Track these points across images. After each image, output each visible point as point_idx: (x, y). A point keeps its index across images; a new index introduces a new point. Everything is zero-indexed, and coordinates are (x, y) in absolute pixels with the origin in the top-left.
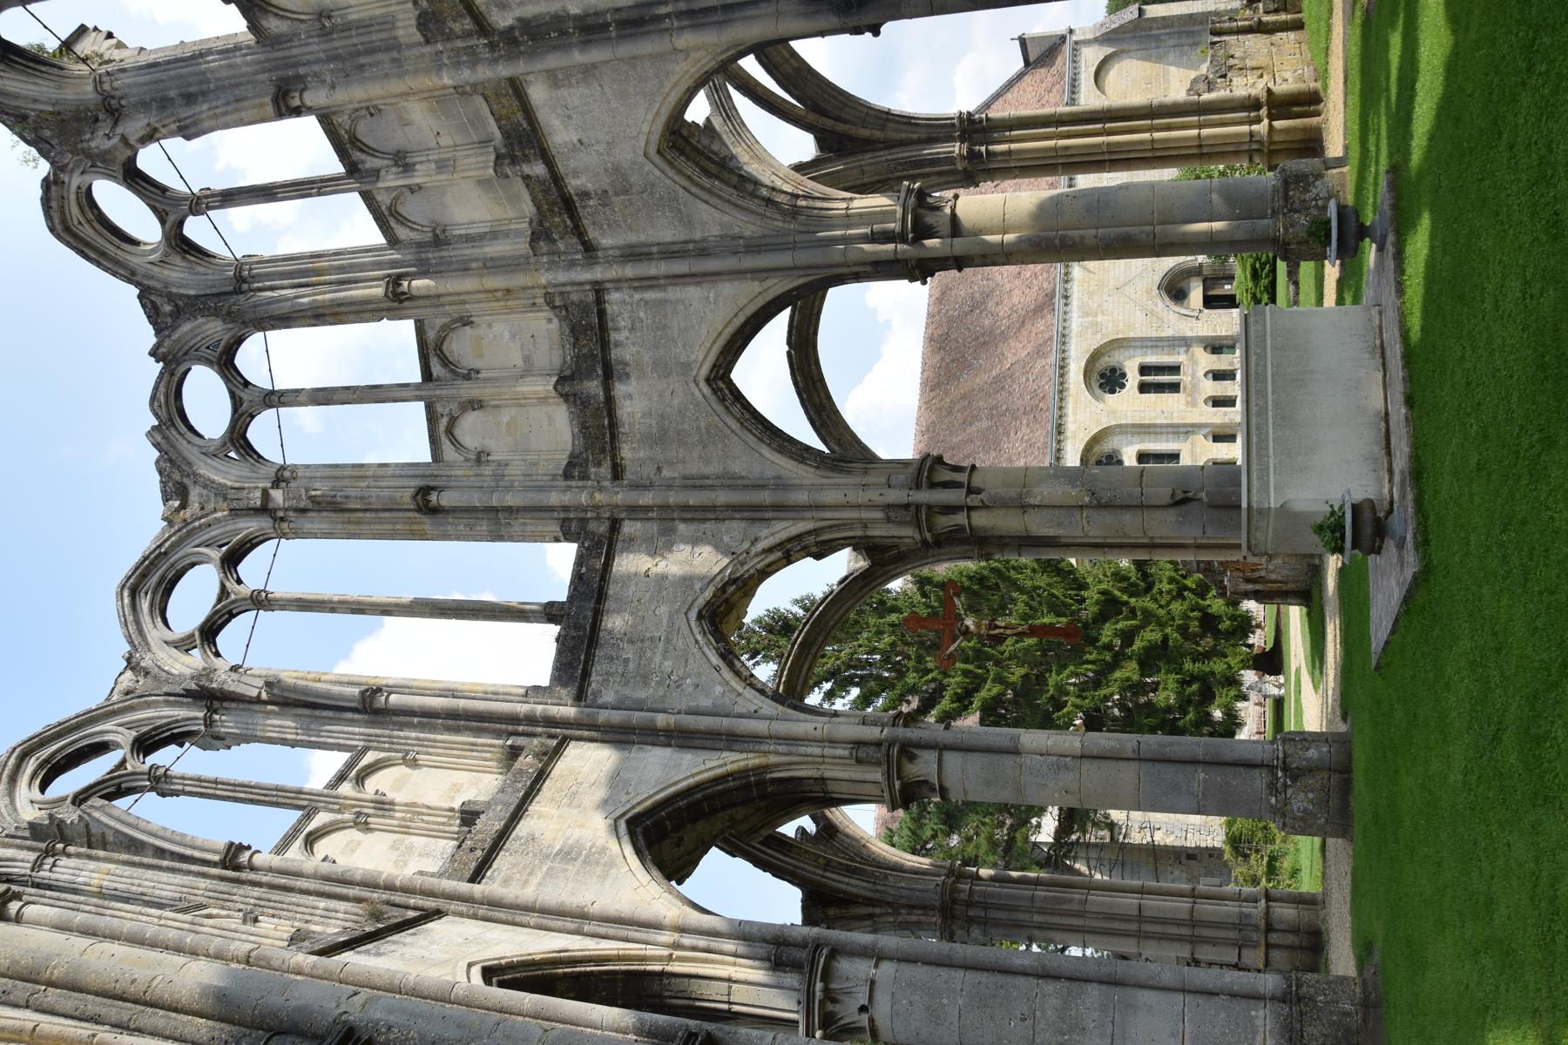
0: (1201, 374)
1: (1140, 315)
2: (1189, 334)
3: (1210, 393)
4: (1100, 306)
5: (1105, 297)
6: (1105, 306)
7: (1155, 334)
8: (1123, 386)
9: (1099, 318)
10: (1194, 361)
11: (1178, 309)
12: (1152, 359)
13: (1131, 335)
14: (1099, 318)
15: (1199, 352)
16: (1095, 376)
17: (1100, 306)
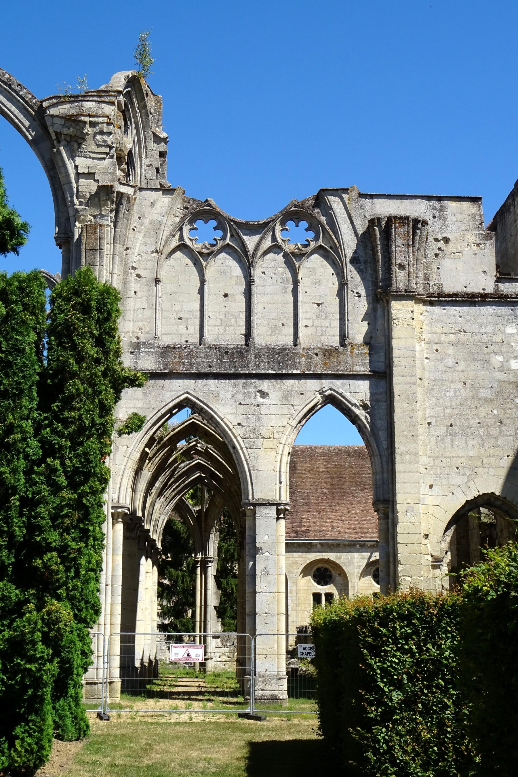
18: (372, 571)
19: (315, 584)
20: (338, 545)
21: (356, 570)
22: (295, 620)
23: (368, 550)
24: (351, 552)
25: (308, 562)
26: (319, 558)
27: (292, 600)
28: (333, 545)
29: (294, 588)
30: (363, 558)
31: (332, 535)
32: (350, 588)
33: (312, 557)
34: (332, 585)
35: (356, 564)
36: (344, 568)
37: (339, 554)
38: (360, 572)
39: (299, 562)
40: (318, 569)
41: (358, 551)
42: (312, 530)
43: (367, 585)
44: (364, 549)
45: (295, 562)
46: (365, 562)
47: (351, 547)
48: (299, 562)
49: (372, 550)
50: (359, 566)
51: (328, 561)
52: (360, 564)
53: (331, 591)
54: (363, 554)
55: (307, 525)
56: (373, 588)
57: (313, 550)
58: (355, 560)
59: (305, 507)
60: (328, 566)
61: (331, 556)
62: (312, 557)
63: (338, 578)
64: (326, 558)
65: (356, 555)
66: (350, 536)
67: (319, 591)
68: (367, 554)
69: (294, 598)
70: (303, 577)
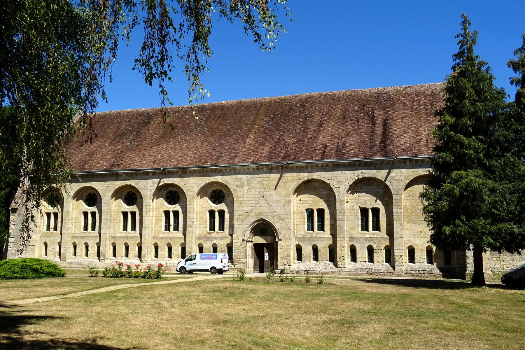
0: (215, 241)
1: (246, 209)
2: (234, 236)
3: (204, 246)
4: (254, 187)
5: (258, 190)
6: (252, 190)
7: (235, 217)
8: (214, 202)
9: (246, 188)
10: (221, 238)
11: (249, 230)
12: (227, 216)
13: (235, 205)
14: (246, 188)
15: (228, 241)
16: (220, 188)
17: (254, 187)
18: (164, 194)
19: (125, 205)
20: (136, 174)
21: (149, 193)
22: (105, 232)
23: (158, 176)
24: (146, 179)
25: (116, 187)
26: (124, 184)
27: (104, 217)
28: (132, 174)
29: (106, 208)
30: (154, 184)
31: (137, 166)
32: (144, 207)
33: (119, 184)
34: (135, 205)
35: (149, 188)
36: (140, 191)
37: (137, 181)
38: (152, 194)
39: (111, 188)
40: (128, 194)
41: (151, 178)
42: (124, 163)
43: (159, 205)
44: (155, 176)
45: (108, 188)
46: (156, 185)
47: (146, 175)
48: (111, 188)
49: (161, 176)
50: (151, 190)
51: (130, 186)
52: (152, 188)
53: (134, 210)
54: (155, 180)
55: (124, 160)
56: (164, 207)
57: (120, 178)
58: (149, 185)
59: (135, 148)
60: (133, 191)
61: (132, 183)
62: (119, 184)
63: (139, 200)
64: (129, 184)
65: (150, 181)
66: (147, 165)
67: (126, 210)
68: (157, 181)
69: (106, 216)
70: (115, 200)
